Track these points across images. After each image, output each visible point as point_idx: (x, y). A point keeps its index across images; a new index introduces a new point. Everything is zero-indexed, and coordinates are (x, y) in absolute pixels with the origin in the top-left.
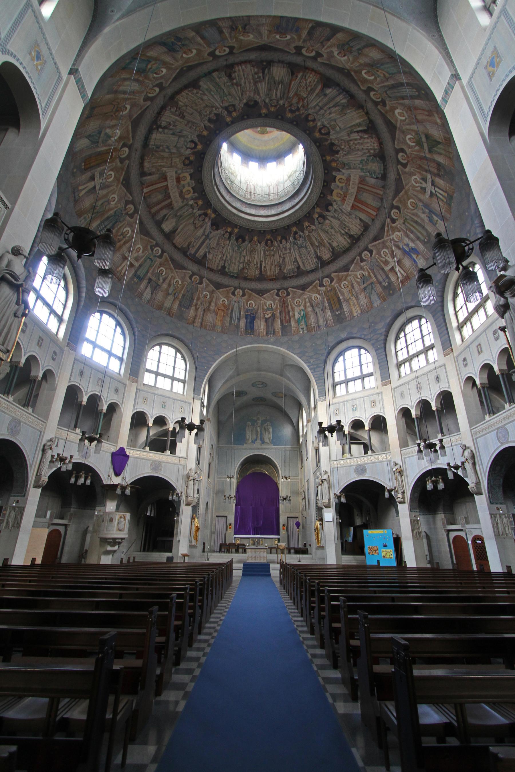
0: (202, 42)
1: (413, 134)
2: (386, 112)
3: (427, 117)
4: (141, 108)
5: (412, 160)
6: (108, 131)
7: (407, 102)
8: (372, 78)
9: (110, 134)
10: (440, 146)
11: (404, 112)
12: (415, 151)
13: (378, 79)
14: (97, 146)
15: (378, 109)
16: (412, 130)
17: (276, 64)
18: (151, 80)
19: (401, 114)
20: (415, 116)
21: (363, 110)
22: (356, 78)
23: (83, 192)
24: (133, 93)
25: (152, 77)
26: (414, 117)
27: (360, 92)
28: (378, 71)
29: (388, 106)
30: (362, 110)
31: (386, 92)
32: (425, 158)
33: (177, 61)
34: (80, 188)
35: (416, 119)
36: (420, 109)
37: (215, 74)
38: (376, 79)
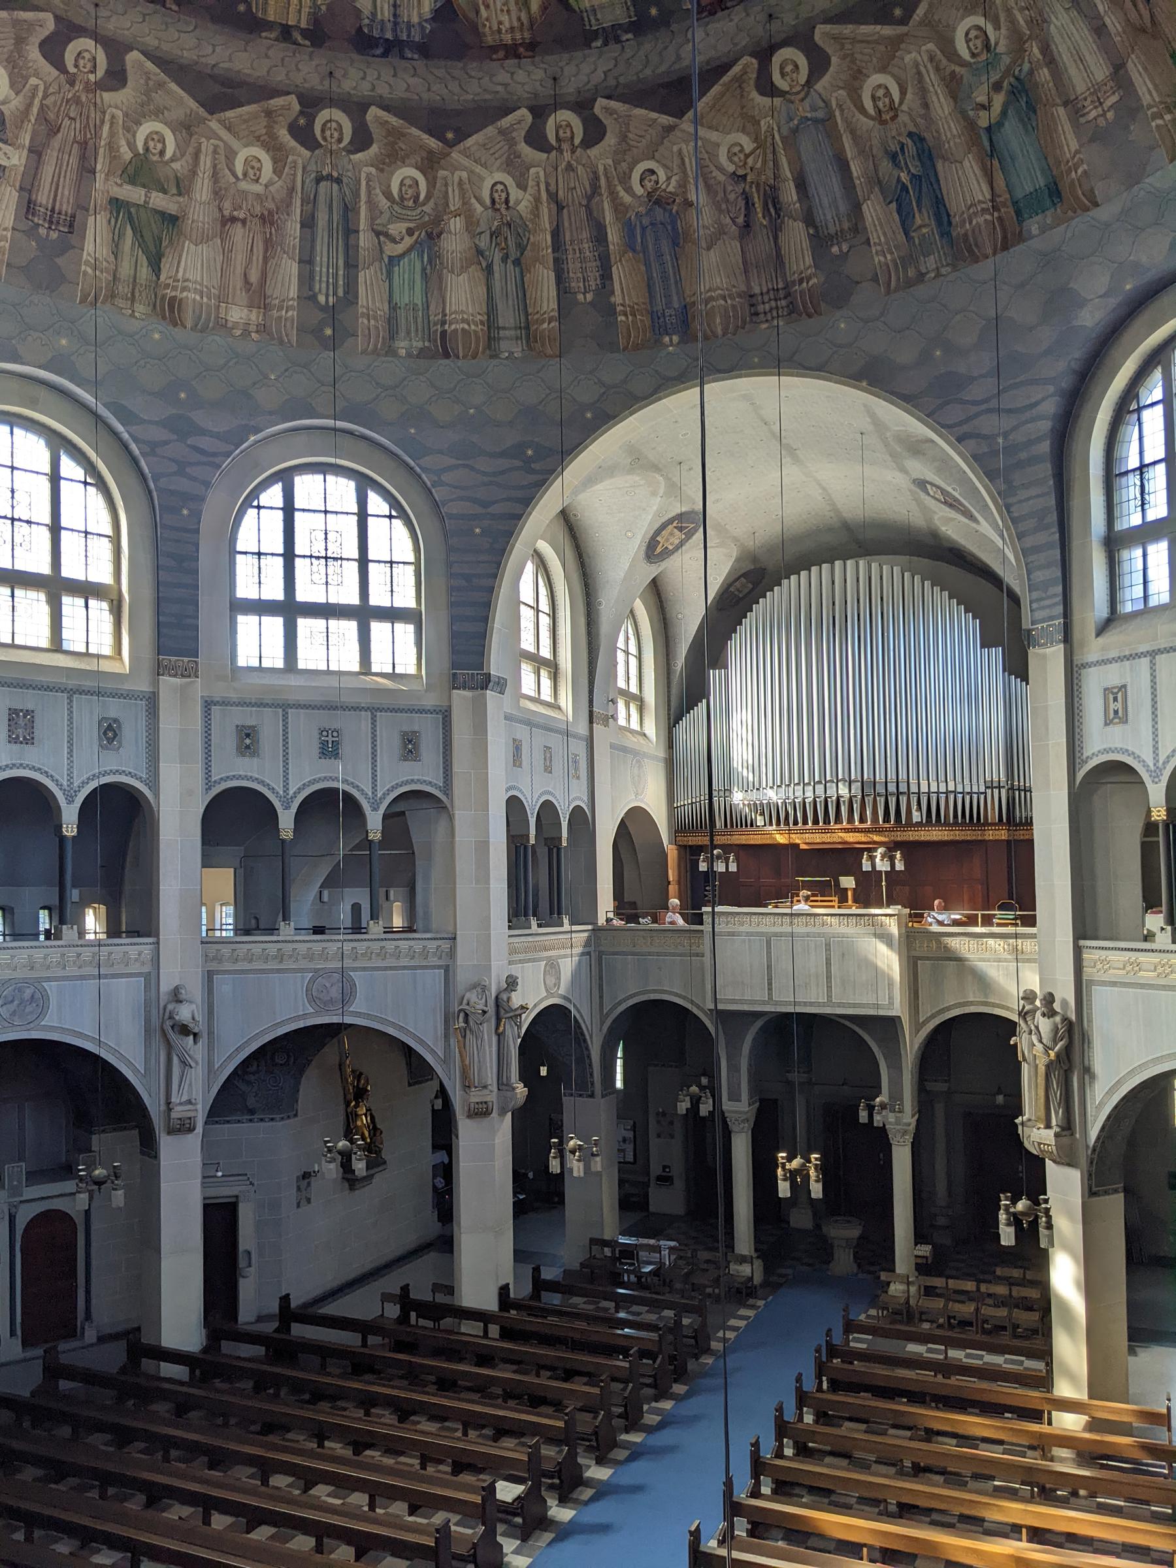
0: (850, 151)
1: (176, 166)
2: (269, 113)
3: (239, 270)
5: (77, 100)
7: (293, 227)
8: (395, 190)
10: (144, 272)
11: (258, 188)
12: (112, 134)
13: (384, 203)
15: (288, 93)
16: (194, 173)
18: (1012, 21)
19: (252, 165)
20: (244, 222)
21: (305, 33)
22: (414, 131)
25: (1003, 31)
26: (242, 216)
27: (365, 89)
28: (410, 232)
30: (303, 25)
31: (338, 181)
32: (87, 170)
33: (917, 65)
35: (233, 219)
36: (266, 260)
38: (388, 195)
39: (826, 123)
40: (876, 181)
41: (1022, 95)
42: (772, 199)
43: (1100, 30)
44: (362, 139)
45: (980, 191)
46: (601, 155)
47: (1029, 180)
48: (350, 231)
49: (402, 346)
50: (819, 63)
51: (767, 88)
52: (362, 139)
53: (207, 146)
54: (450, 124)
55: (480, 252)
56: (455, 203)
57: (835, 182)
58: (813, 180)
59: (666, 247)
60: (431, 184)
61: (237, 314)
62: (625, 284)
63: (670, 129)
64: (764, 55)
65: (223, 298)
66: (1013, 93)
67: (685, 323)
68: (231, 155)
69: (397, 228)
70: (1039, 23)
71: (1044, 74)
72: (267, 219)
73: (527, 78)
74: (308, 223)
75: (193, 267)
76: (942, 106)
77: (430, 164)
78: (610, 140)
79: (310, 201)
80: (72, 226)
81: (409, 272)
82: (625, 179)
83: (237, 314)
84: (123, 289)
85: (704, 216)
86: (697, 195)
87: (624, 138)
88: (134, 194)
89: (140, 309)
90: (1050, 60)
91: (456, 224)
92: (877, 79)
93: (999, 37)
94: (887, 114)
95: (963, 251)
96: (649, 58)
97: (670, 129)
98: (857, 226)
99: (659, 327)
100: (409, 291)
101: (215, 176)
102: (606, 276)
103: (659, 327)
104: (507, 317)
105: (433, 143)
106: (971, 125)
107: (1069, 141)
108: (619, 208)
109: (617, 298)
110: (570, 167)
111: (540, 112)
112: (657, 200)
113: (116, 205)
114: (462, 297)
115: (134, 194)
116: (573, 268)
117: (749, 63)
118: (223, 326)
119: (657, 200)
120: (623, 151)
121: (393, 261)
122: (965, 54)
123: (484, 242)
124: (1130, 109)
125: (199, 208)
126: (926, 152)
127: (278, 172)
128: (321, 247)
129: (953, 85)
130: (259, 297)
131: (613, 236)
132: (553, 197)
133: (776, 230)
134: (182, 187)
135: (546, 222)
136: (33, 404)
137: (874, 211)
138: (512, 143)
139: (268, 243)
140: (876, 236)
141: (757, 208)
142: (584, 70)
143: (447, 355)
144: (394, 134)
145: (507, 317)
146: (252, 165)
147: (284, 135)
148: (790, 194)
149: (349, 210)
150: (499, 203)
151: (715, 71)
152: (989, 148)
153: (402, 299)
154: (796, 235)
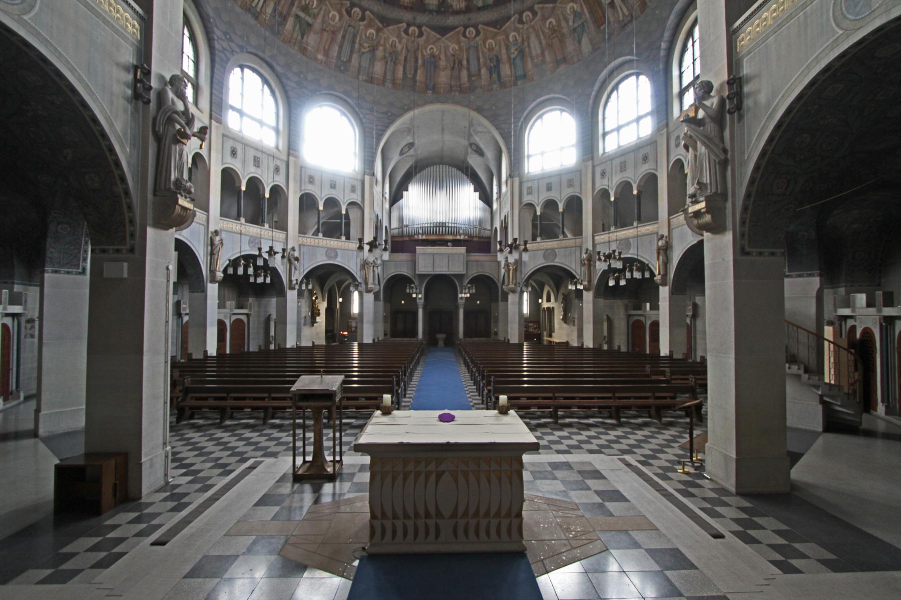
0: (481, 56)
4: (543, 8)
6: (571, 23)
7: (340, 37)
9: (572, 17)
10: (299, 38)
11: (333, 23)
14: (586, 21)
16: (318, 14)
17: (435, 8)
19: (334, 16)
23: (625, 10)
24: (538, 36)
29: (344, 13)
34: (621, 18)
37: (480, 4)
39: (477, 48)
40: (485, 64)
41: (521, 52)
42: (460, 62)
43: (540, 43)
44: (363, 19)
45: (509, 73)
46: (421, 41)
47: (520, 72)
48: (354, 42)
49: (361, 77)
50: (478, 33)
51: (464, 35)
52: (363, 19)
53: (324, 8)
54: (386, 22)
55: (385, 57)
56: (382, 42)
57: (476, 62)
58: (471, 61)
59: (432, 68)
60: (377, 35)
61: (320, 57)
62: (420, 76)
63: (439, 39)
64: (466, 27)
65: (318, 51)
66: (520, 52)
67: (434, 89)
68: (329, 12)
69: (366, 45)
70: (528, 38)
71: (527, 50)
72: (334, 33)
73: (408, 16)
74: (344, 37)
75: (312, 39)
76: (504, 51)
77: (378, 30)
78: (424, 37)
79: (346, 31)
80: (285, 19)
81: (367, 56)
82: (426, 48)
83: (320, 57)
84: (293, 41)
85: (443, 63)
86: (443, 57)
87: (427, 38)
88: (302, 15)
89: (296, 48)
90: (529, 46)
91: (381, 48)
92: (490, 41)
93: (519, 39)
94: (491, 49)
95: (503, 85)
96: (439, 20)
97: (439, 39)
98: (479, 74)
99: (427, 88)
100: (365, 64)
101: (324, 16)
102: (416, 71)
103: (427, 88)
104: (389, 76)
105: (381, 25)
106: (509, 58)
107: (530, 65)
108: (423, 55)
109: (418, 78)
110: (413, 42)
111: (409, 25)
112: (432, 56)
113: (297, 16)
114: (378, 68)
115: (302, 15)
116: (408, 69)
117: (461, 29)
118: (316, 59)
119: (432, 56)
120: (427, 42)
121: (363, 53)
122: (511, 39)
123: (387, 55)
124: (544, 61)
125: (318, 24)
126: (498, 61)
127: (339, 21)
128: (345, 44)
129: (507, 47)
130: (327, 54)
131: (420, 62)
132: (407, 47)
133: (460, 70)
134: (315, 17)
135: (404, 54)
136: (261, 67)
137: (484, 71)
138: (400, 31)
139: (332, 39)
140: (483, 77)
141: (456, 64)
142: (422, 18)
143: (371, 83)
144: (371, 20)
145: (389, 76)
146: (334, 16)
147: (344, 10)
148: (465, 63)
149: (355, 37)
150: (393, 46)
151: (453, 28)
152: (512, 62)
153: (363, 64)
154: (464, 73)
